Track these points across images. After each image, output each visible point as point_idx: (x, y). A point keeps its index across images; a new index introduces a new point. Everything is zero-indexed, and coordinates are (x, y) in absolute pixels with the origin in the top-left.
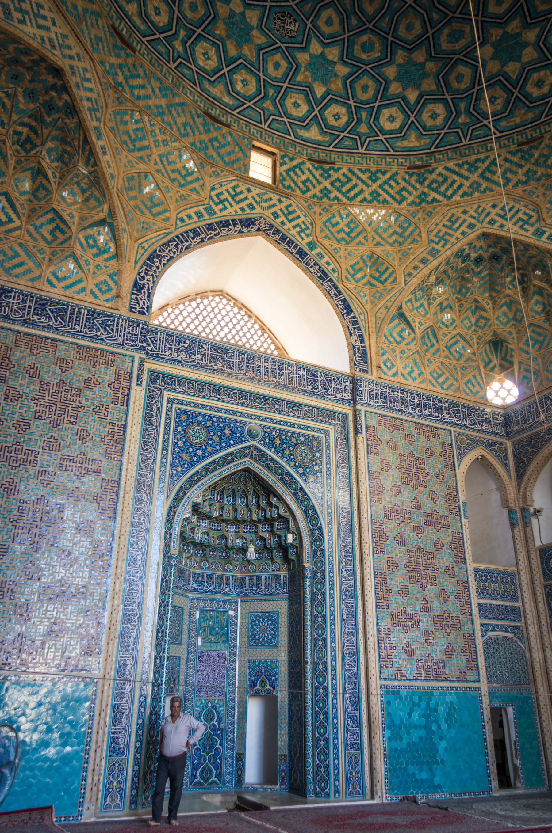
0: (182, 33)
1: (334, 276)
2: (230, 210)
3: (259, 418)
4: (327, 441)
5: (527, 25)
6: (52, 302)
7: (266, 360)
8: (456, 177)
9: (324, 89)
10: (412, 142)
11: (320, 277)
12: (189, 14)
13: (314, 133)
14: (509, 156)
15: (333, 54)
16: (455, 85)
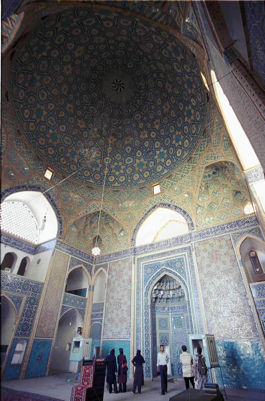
0: (129, 178)
1: (179, 206)
2: (150, 207)
3: (164, 259)
4: (185, 257)
5: (188, 106)
6: (117, 253)
7: (163, 242)
8: (196, 156)
9: (164, 159)
10: (186, 154)
11: (175, 209)
12: (129, 173)
13: (166, 171)
14: (203, 140)
15: (162, 150)
16: (186, 132)
